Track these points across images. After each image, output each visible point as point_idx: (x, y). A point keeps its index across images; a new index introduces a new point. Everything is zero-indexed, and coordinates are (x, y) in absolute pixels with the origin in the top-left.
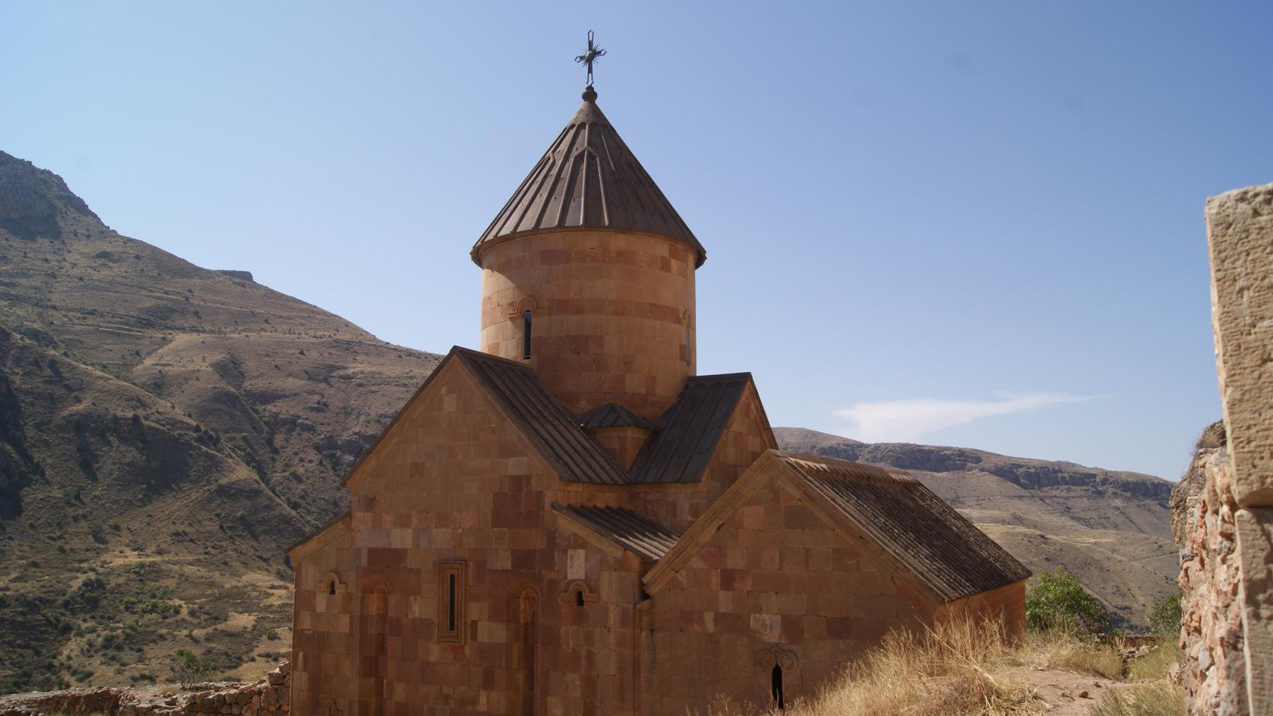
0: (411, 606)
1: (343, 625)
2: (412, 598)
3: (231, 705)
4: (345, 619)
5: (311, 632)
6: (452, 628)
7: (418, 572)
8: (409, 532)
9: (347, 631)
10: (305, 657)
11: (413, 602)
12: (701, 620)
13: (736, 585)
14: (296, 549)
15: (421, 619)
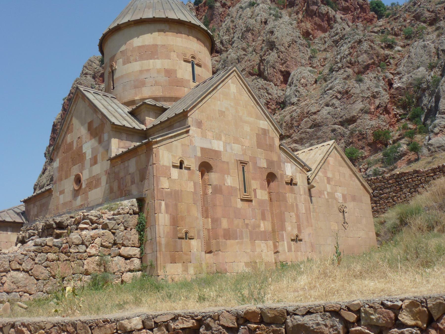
0: (226, 180)
1: (190, 187)
2: (226, 176)
3: (77, 245)
4: (192, 183)
5: (169, 190)
6: (245, 192)
7: (228, 163)
8: (221, 143)
9: (193, 191)
10: (166, 205)
11: (226, 178)
12: (324, 194)
13: (331, 183)
14: (158, 139)
15: (231, 187)
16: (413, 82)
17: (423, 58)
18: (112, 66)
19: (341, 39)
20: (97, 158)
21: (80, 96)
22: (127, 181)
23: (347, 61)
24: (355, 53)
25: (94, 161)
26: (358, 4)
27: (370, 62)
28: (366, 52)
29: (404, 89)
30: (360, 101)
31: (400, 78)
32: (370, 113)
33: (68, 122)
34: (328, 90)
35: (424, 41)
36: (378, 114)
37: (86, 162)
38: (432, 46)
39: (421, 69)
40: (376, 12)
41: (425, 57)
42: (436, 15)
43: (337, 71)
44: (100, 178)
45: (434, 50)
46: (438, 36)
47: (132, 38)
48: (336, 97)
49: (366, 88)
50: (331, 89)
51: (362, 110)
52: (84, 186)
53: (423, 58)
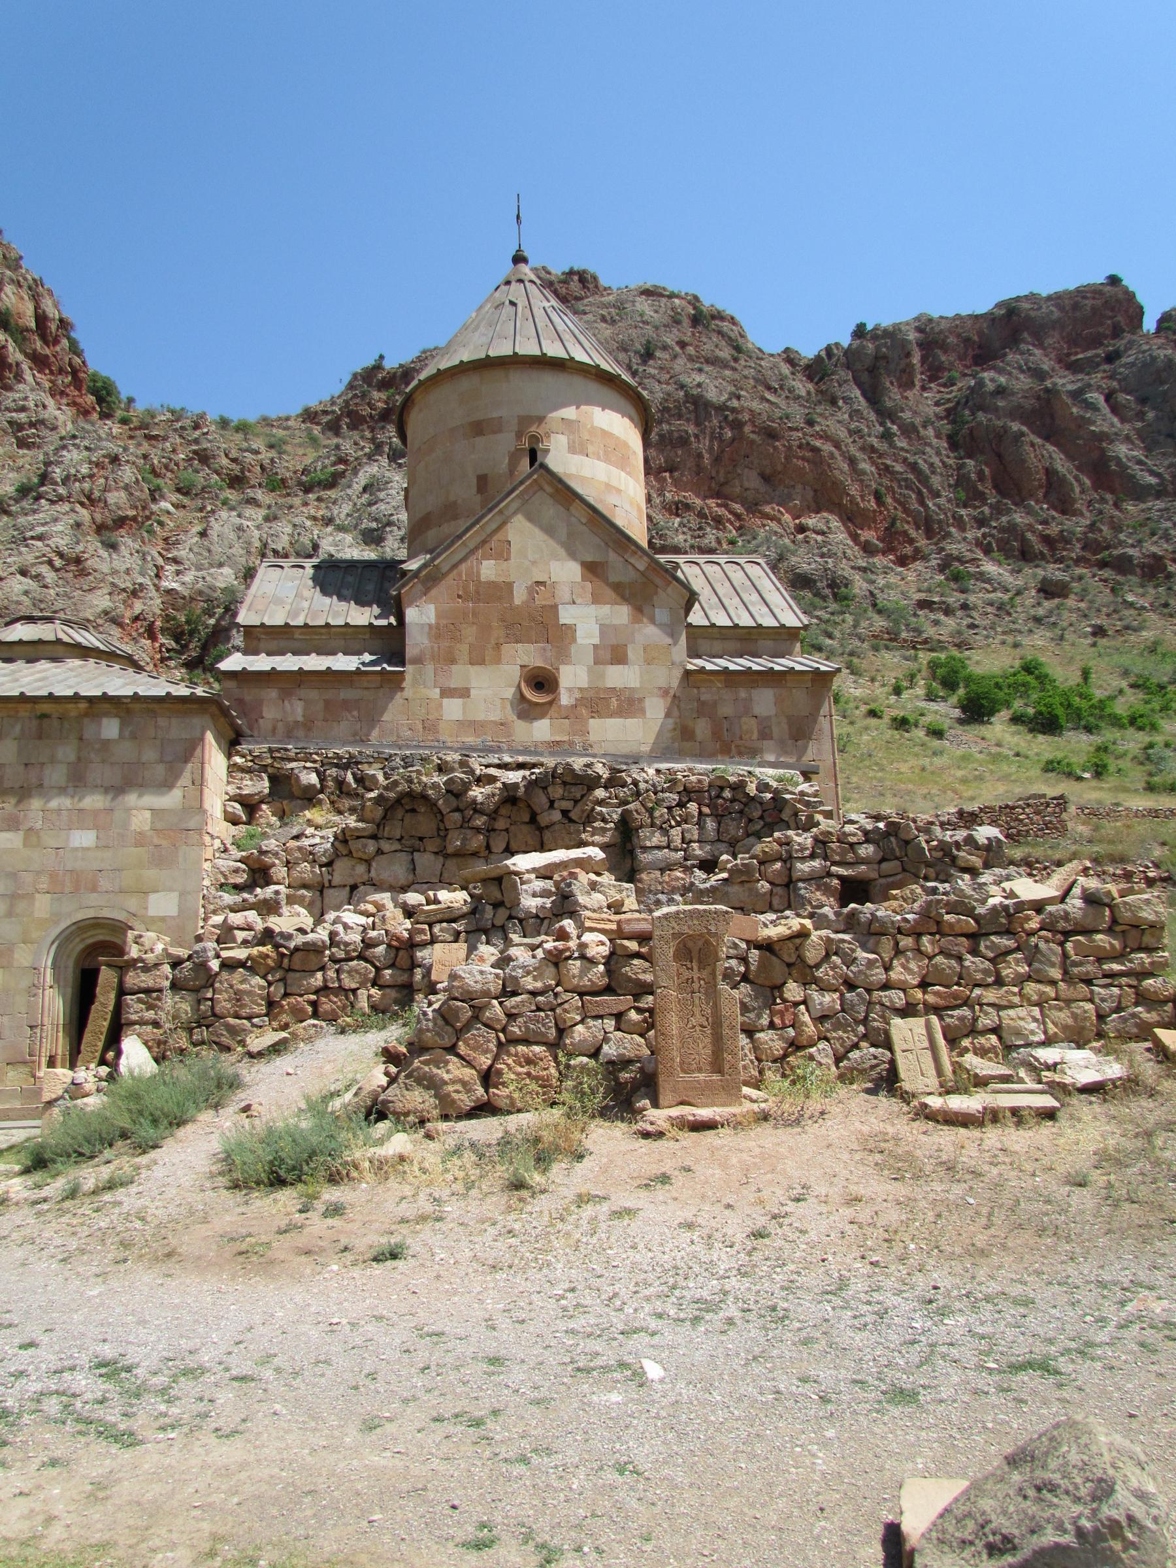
16: (207, 591)
17: (233, 551)
18: (535, 439)
19: (32, 425)
20: (626, 655)
21: (549, 489)
22: (745, 727)
23: (82, 491)
24: (102, 481)
25: (618, 656)
26: (70, 365)
27: (131, 513)
28: (126, 487)
29: (184, 598)
30: (106, 591)
31: (178, 573)
32: (120, 625)
33: (489, 530)
34: (32, 538)
35: (239, 516)
36: (134, 634)
37: (573, 648)
38: (256, 533)
39: (226, 570)
40: (100, 400)
41: (237, 550)
42: (242, 471)
43: (52, 502)
44: (641, 700)
45: (258, 544)
46: (267, 519)
47: (589, 403)
48: (50, 563)
49: (123, 568)
50: (40, 538)
51: (106, 613)
52: (565, 699)
53: (233, 551)
